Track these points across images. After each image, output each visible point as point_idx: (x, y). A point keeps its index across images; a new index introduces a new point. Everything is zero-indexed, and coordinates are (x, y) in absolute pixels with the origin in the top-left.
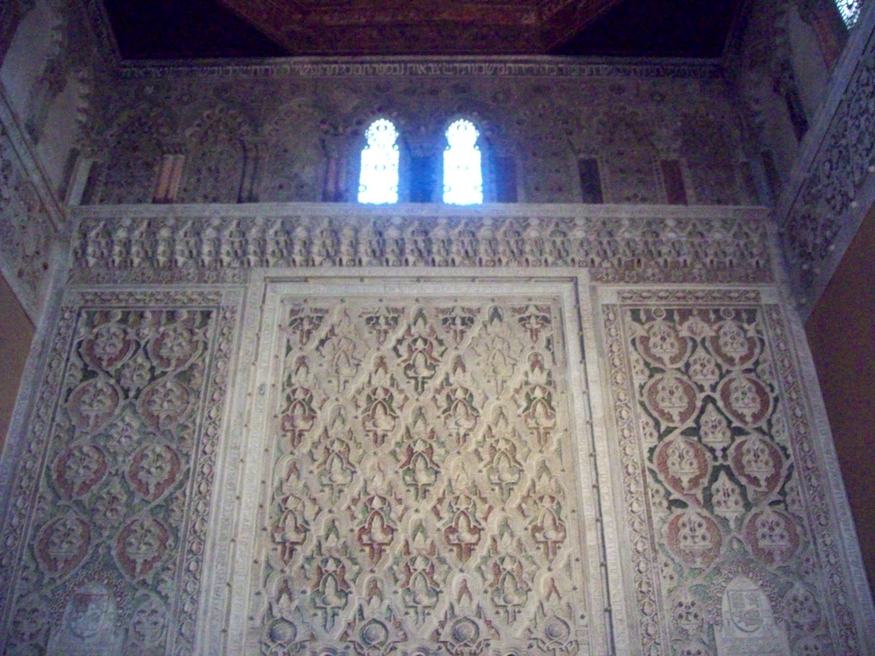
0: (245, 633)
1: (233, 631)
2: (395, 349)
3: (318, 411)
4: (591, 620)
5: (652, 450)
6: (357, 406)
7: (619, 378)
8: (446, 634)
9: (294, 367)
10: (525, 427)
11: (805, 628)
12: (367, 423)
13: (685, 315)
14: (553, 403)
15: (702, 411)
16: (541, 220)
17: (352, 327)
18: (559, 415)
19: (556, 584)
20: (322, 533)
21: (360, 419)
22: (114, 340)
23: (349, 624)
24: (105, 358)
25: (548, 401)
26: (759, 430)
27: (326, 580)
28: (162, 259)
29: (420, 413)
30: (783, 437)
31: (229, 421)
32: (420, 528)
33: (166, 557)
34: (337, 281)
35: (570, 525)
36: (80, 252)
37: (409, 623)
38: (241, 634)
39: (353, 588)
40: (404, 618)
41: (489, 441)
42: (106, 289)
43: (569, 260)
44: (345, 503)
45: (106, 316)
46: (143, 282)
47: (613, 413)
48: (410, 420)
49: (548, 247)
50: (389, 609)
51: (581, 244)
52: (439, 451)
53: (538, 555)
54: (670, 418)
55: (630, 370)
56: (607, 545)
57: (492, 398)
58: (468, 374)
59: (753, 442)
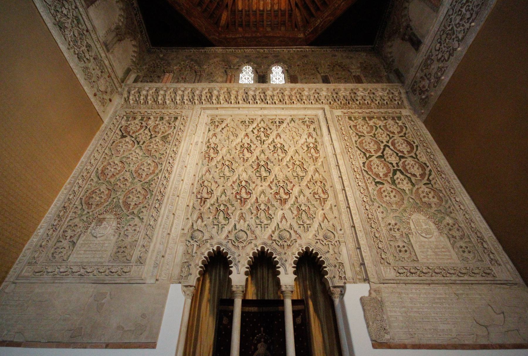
1: (173, 234)
2: (252, 131)
3: (220, 151)
5: (364, 163)
7: (346, 138)
8: (275, 236)
9: (211, 137)
11: (458, 238)
13: (371, 118)
15: (384, 150)
16: (309, 89)
17: (235, 124)
19: (326, 216)
20: (219, 194)
22: (137, 126)
23: (229, 232)
24: (132, 132)
25: (316, 148)
26: (412, 157)
27: (219, 213)
28: (160, 102)
29: (263, 152)
30: (424, 159)
31: (181, 153)
32: (263, 192)
33: (145, 203)
34: (230, 109)
36: (127, 99)
37: (258, 231)
38: (177, 236)
39: (232, 217)
41: (292, 161)
42: (136, 111)
43: (321, 102)
44: (230, 183)
45: (135, 118)
46: (152, 108)
47: (345, 150)
48: (258, 154)
49: (312, 98)
50: (248, 225)
51: (325, 97)
53: (317, 204)
54: (370, 152)
55: (350, 136)
57: (292, 146)
58: (282, 139)
59: (410, 161)
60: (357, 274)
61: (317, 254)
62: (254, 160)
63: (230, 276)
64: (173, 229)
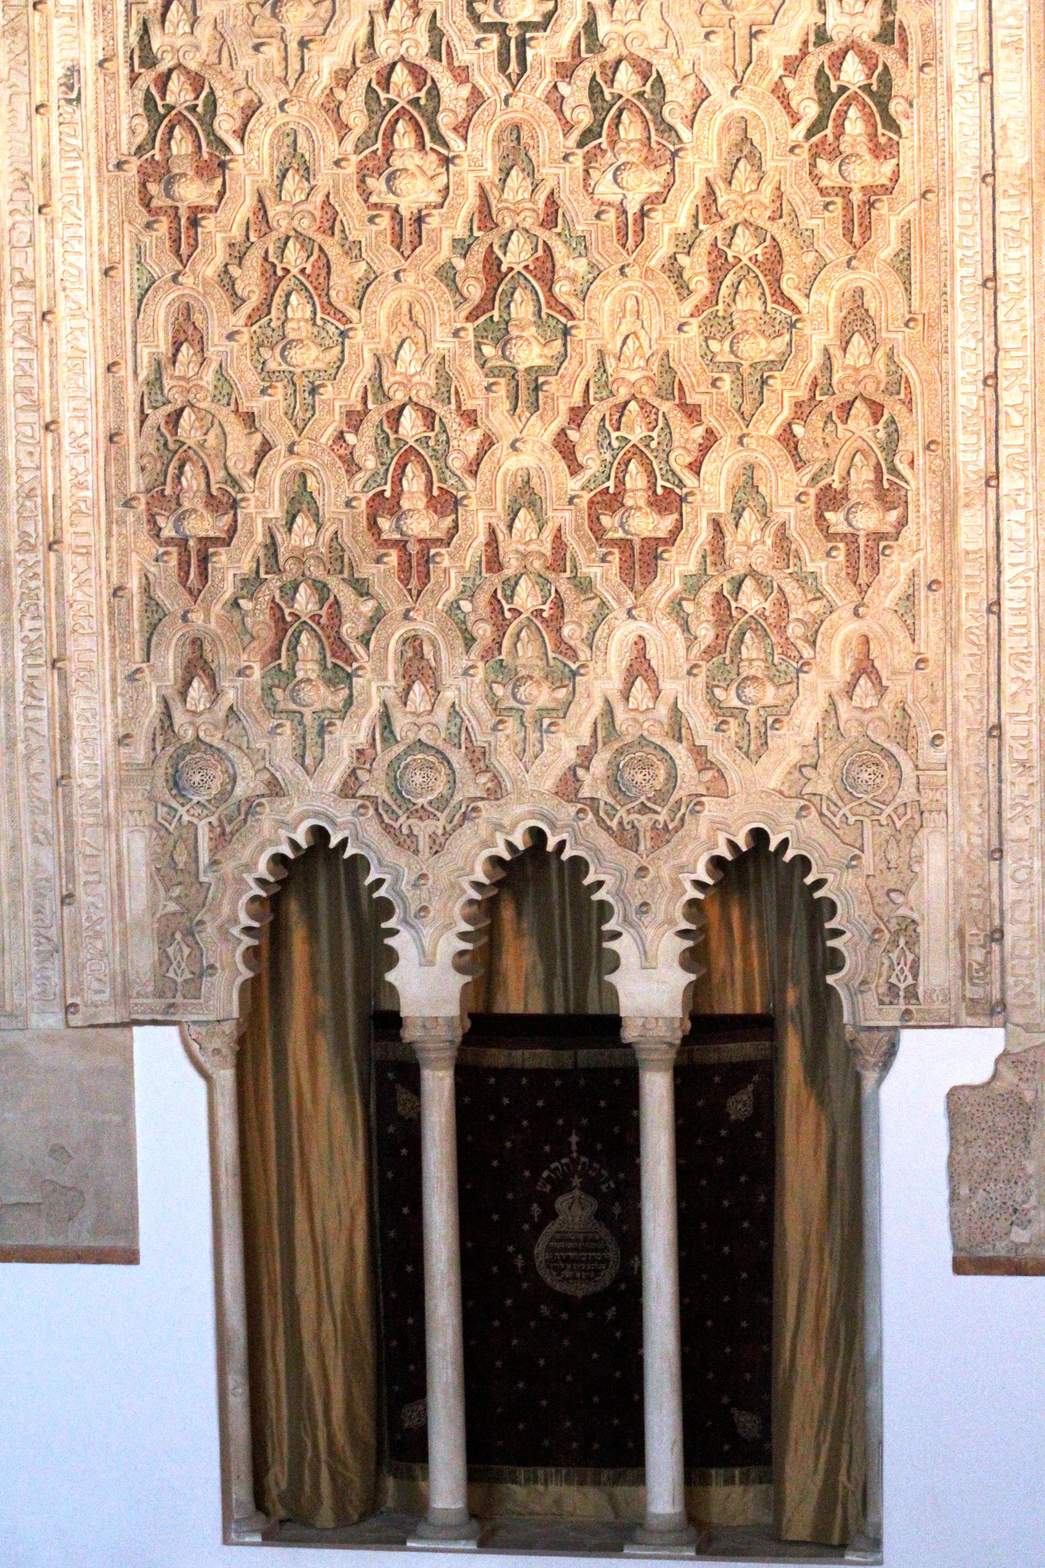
0: (111, 779)
4: (955, 753)
6: (343, 129)
8: (593, 782)
10: (809, 189)
12: (370, 182)
14: (895, 107)
18: (909, 146)
20: (276, 511)
21: (351, 168)
25: (880, 94)
32: (526, 496)
35: (917, 483)
37: (505, 761)
38: (104, 786)
40: (491, 739)
48: (490, 170)
50: (454, 711)
52: (571, 265)
56: (1006, 558)
57: (719, 90)
60: (966, 973)
61: (803, 864)
62: (461, 232)
63: (391, 977)
64: (76, 750)
